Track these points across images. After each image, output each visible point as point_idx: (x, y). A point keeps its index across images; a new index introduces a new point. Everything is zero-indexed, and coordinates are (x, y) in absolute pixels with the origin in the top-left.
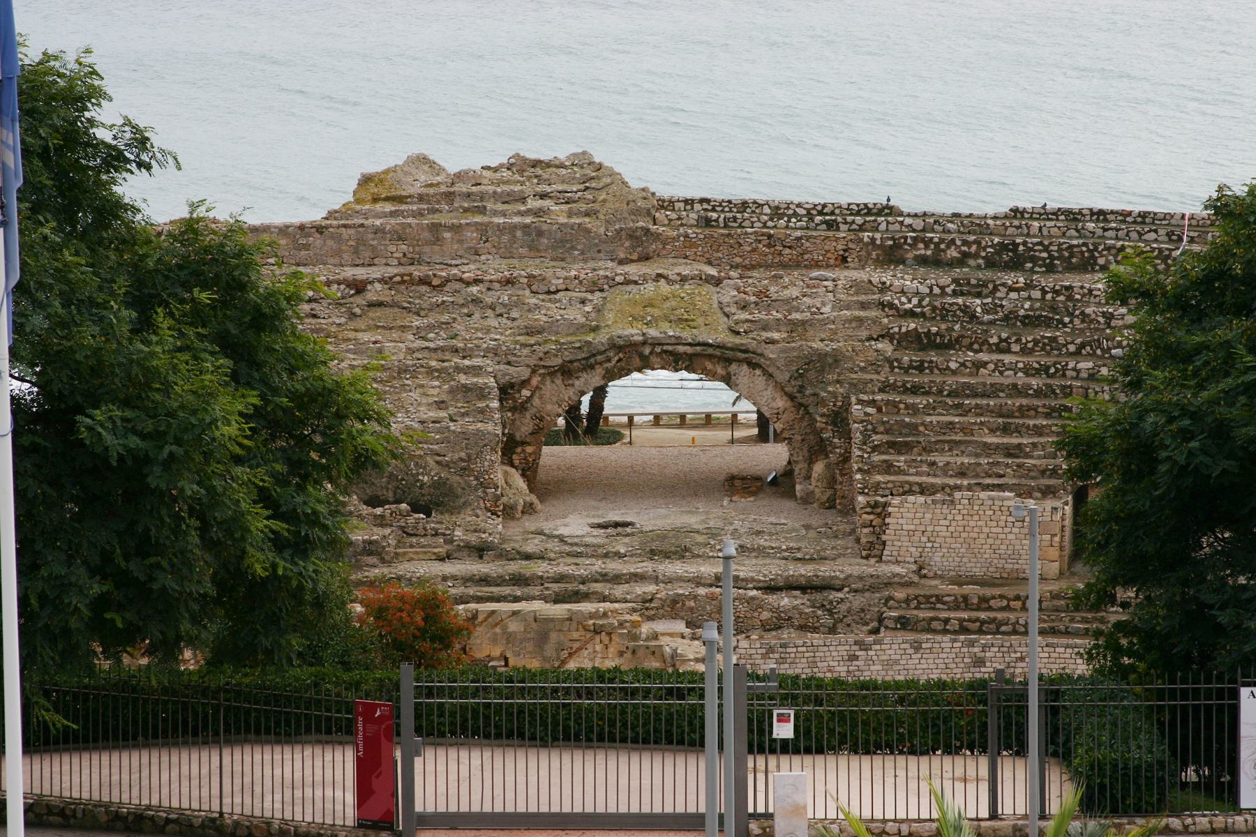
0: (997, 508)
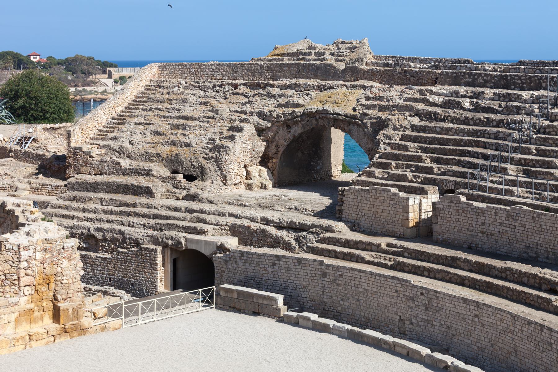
0: (385, 195)
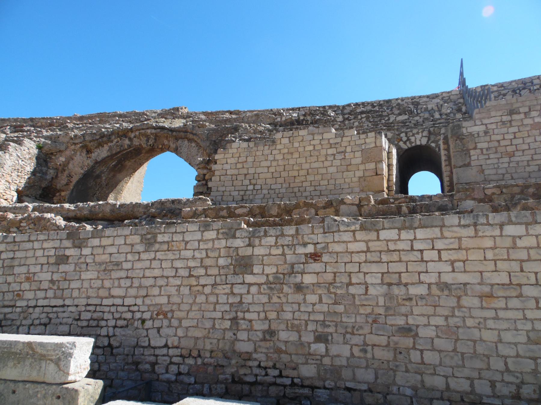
0: (317, 142)
